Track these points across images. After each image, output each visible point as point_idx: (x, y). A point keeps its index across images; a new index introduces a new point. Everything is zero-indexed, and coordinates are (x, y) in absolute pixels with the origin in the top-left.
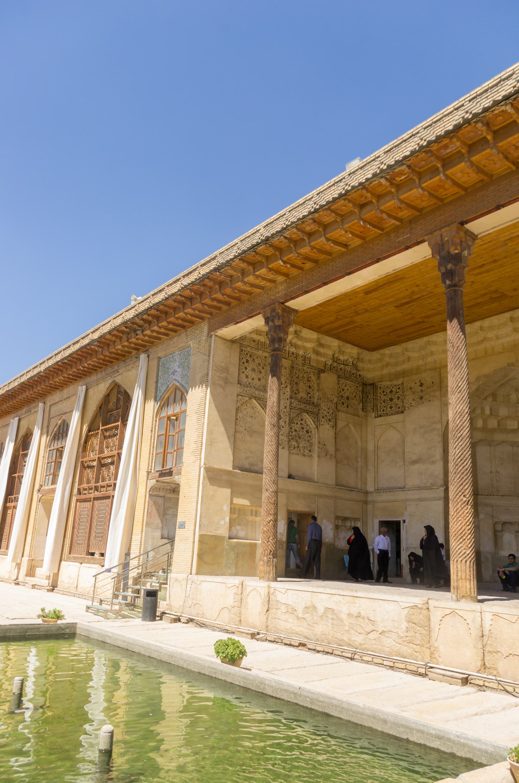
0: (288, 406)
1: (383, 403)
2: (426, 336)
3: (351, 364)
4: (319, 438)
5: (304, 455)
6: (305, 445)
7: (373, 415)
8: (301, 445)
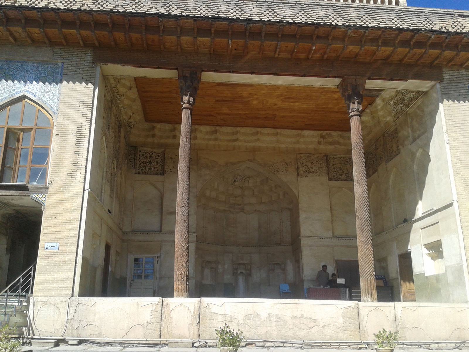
1: (142, 164)
7: (134, 171)
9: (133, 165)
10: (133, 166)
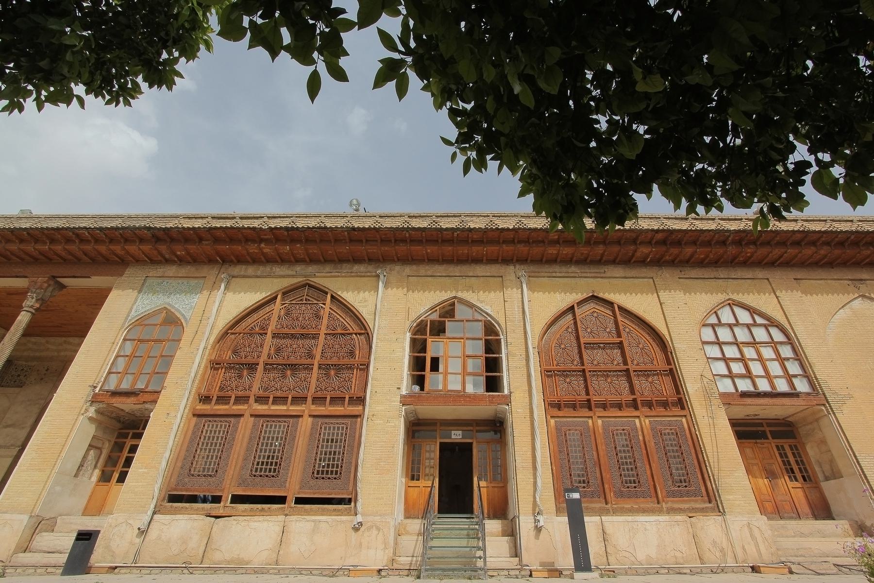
2: (65, 337)
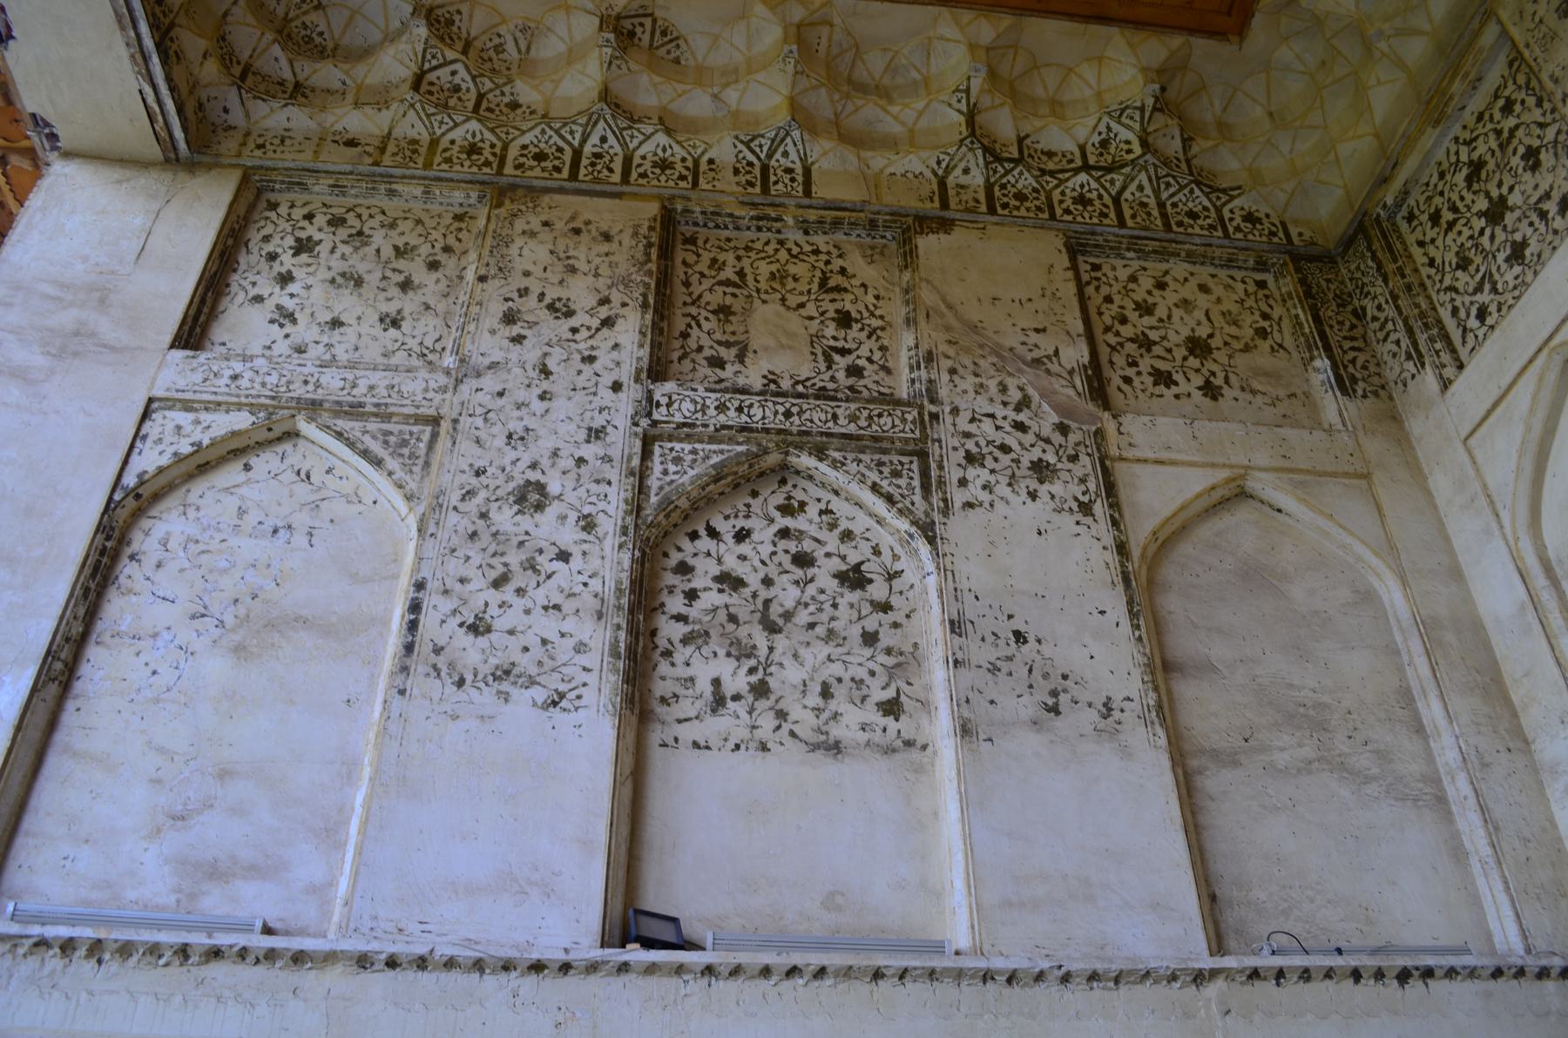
0: (622, 420)
3: (1138, 150)
4: (952, 592)
5: (836, 748)
6: (836, 669)
7: (1429, 379)
8: (786, 677)
9: (1406, 342)
10: (1409, 357)
